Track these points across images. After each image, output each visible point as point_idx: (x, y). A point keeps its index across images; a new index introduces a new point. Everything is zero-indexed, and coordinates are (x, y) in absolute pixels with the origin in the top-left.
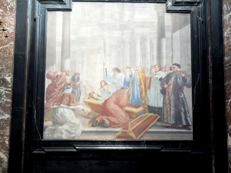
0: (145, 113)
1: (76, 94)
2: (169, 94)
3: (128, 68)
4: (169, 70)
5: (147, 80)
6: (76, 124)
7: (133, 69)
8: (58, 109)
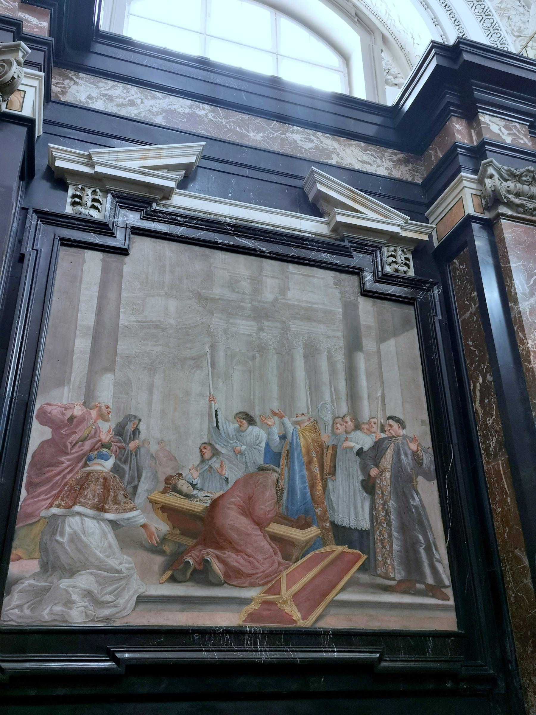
0: (325, 544)
1: (127, 476)
2: (383, 493)
3: (274, 414)
4: (379, 431)
8: (64, 522)
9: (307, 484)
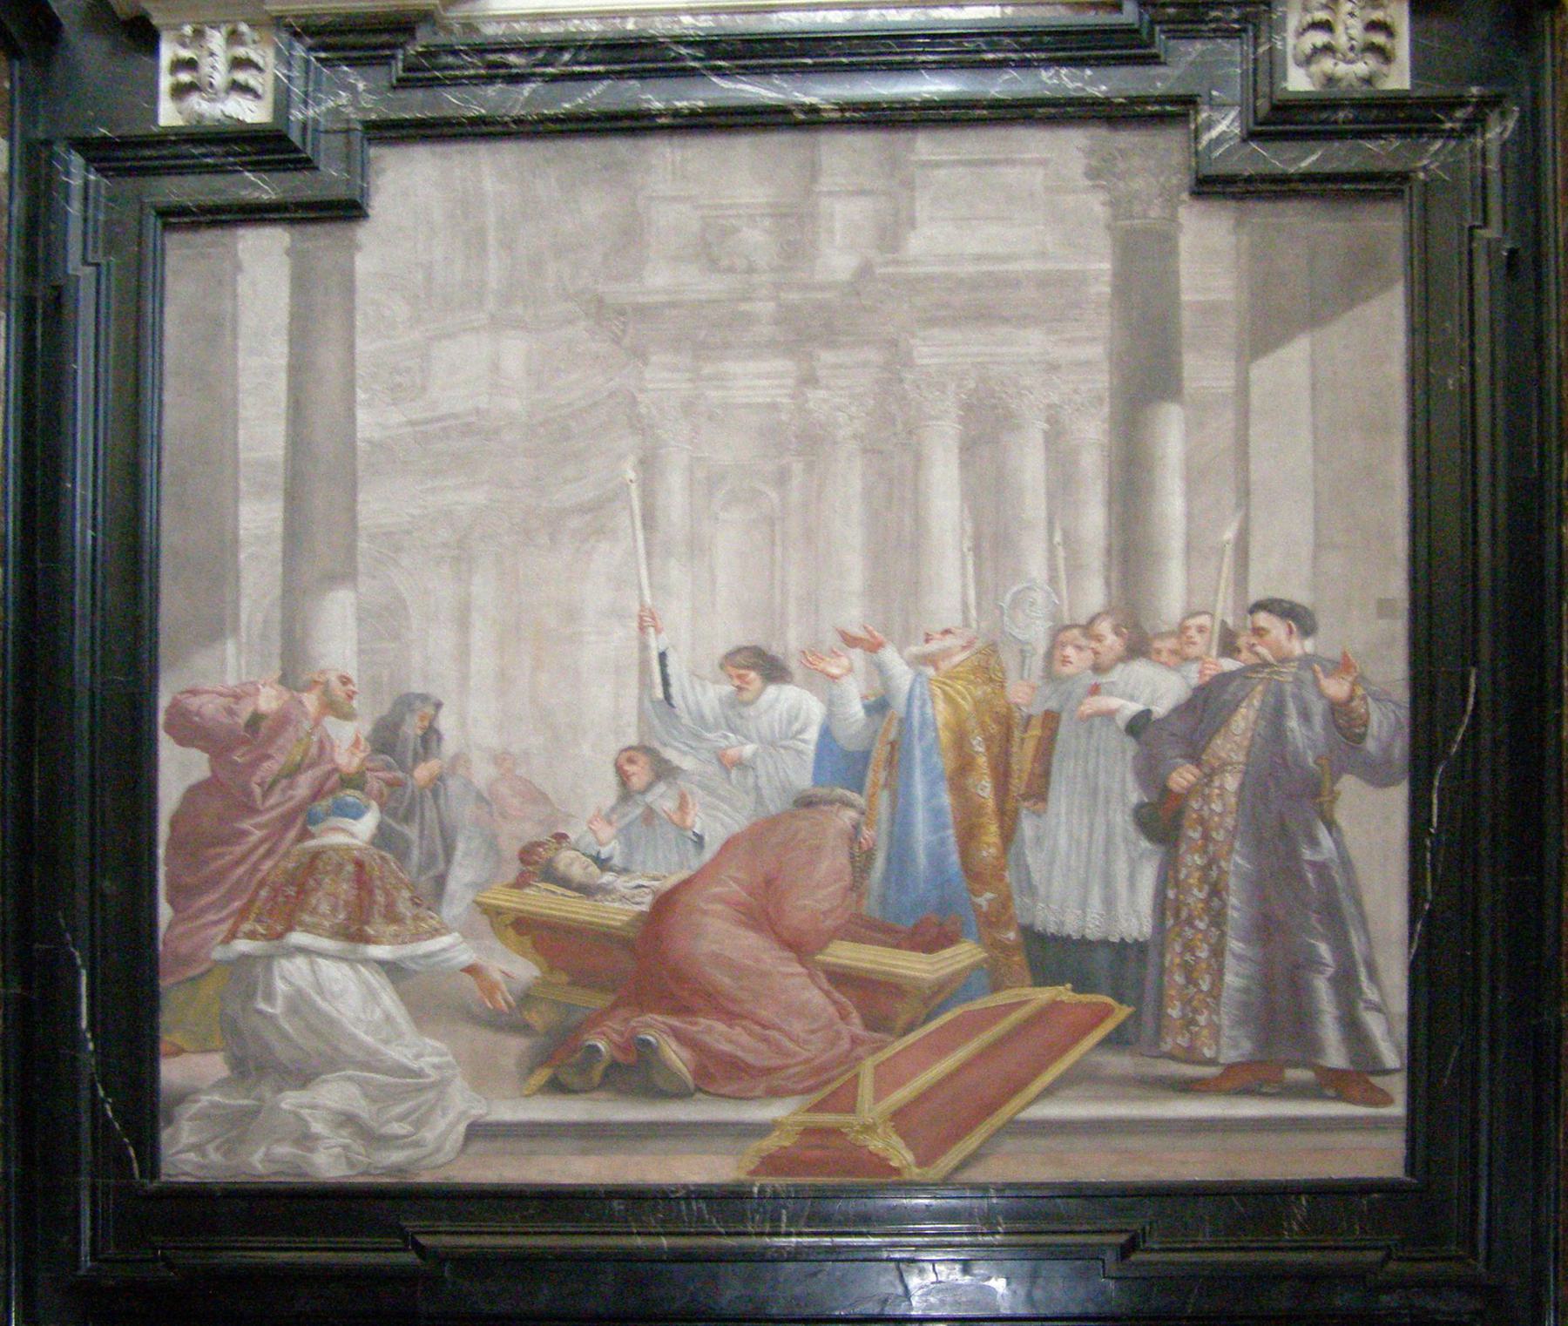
0: (996, 988)
2: (1206, 837)
3: (850, 641)
5: (1017, 734)
6: (419, 1074)
7: (900, 651)
8: (269, 969)
9: (951, 832)
